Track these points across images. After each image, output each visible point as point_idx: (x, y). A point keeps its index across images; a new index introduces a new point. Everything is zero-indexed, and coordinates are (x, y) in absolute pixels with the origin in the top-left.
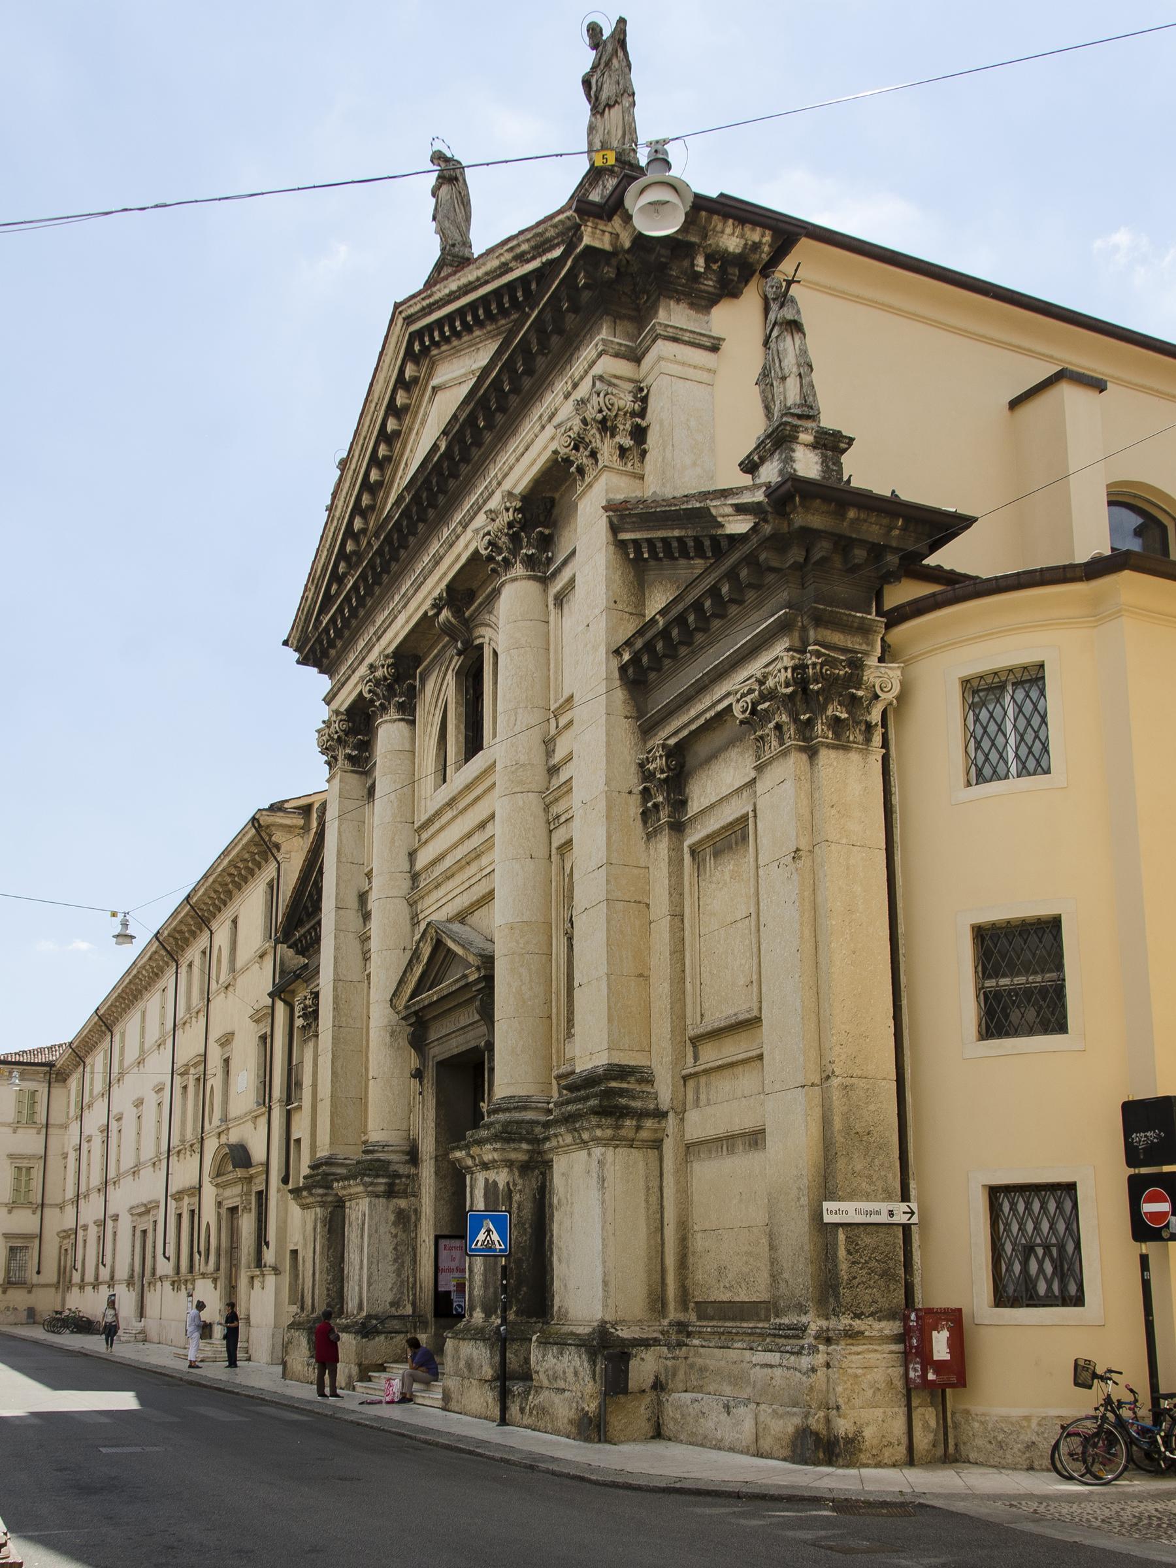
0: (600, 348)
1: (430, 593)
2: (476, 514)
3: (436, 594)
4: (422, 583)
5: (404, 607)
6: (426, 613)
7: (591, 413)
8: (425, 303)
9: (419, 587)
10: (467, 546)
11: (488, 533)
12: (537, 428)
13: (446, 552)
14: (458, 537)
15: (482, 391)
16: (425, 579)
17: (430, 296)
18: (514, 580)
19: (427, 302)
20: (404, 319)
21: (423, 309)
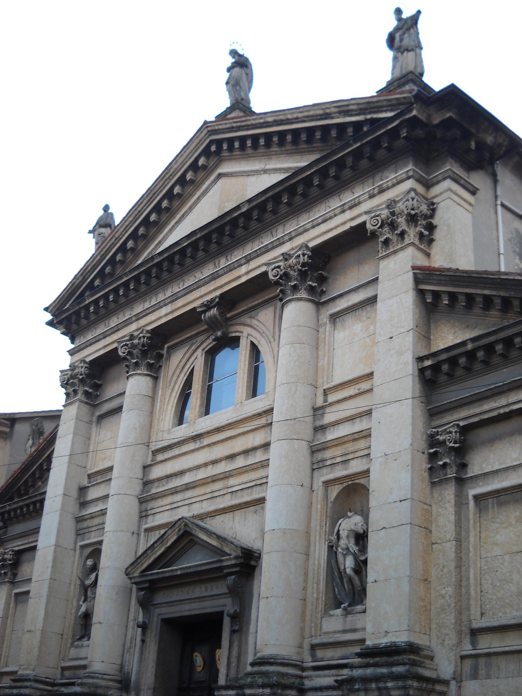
1: (201, 297)
3: (209, 298)
6: (194, 309)
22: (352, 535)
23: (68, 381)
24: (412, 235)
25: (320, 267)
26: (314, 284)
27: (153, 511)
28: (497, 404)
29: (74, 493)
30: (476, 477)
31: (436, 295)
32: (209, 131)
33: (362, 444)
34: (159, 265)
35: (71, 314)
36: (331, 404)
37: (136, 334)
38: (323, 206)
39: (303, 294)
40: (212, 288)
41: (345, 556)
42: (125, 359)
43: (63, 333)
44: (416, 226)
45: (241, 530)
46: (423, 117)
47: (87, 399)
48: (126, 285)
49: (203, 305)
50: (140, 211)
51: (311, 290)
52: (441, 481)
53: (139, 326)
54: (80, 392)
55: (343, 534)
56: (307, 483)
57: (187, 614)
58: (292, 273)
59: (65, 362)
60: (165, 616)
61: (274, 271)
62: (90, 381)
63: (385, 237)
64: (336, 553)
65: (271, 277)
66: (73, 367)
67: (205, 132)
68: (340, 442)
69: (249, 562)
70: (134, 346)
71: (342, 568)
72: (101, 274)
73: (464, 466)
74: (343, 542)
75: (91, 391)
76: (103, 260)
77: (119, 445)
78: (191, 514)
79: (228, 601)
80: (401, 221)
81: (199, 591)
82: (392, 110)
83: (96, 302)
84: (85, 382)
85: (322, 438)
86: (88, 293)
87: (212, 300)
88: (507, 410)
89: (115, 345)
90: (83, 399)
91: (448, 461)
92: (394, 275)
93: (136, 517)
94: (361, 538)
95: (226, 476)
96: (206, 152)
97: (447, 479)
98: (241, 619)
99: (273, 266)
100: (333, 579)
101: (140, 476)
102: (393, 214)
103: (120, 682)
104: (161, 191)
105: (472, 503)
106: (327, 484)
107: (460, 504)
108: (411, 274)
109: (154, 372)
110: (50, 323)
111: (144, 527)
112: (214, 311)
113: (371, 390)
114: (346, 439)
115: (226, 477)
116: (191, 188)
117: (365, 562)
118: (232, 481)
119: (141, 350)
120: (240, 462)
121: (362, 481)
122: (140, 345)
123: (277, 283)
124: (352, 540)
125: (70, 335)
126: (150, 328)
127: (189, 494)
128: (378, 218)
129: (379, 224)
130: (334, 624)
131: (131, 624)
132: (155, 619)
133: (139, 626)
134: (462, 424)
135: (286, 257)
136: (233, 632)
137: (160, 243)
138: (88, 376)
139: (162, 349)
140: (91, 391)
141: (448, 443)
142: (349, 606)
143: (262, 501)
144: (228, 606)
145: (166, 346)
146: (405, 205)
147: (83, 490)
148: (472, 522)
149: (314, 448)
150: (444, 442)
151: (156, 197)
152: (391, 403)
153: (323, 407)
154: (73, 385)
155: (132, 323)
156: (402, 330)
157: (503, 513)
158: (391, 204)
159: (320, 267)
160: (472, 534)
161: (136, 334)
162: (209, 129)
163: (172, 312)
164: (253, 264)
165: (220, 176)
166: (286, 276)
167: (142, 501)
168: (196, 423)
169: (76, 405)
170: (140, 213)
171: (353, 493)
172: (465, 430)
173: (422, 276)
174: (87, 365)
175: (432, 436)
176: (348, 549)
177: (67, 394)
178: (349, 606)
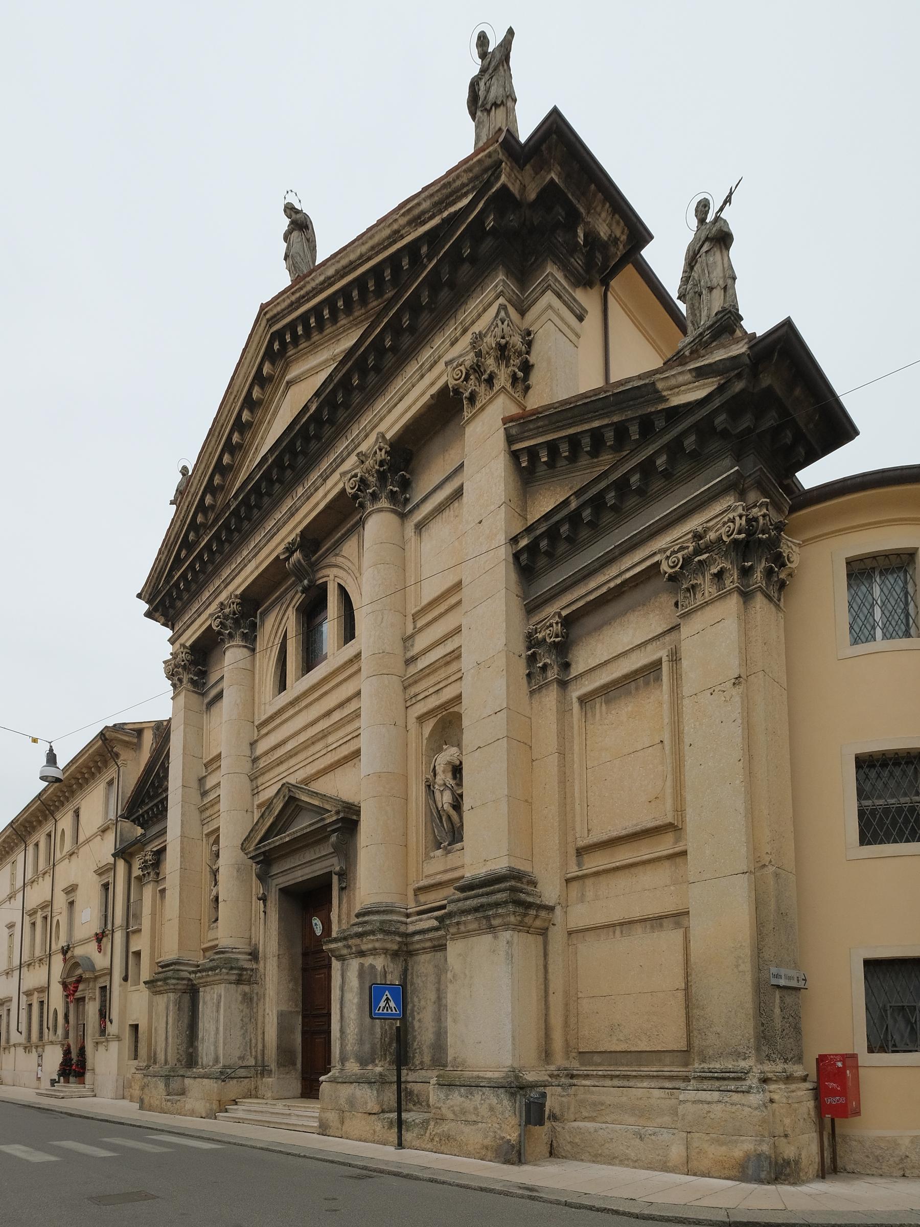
0: (500, 288)
1: (283, 540)
2: (349, 455)
3: (290, 539)
4: (275, 534)
6: (278, 557)
7: (490, 341)
8: (293, 298)
9: (272, 537)
10: (326, 495)
11: (355, 476)
12: (417, 376)
13: (303, 504)
14: (316, 490)
15: (362, 349)
16: (278, 530)
17: (301, 289)
18: (380, 510)
19: (298, 295)
20: (268, 320)
21: (292, 303)
22: (450, 768)
23: (173, 672)
24: (503, 378)
25: (402, 462)
26: (395, 489)
27: (263, 787)
29: (194, 784)
30: (581, 675)
31: (532, 452)
33: (454, 667)
35: (166, 597)
38: (399, 378)
39: (384, 503)
41: (442, 792)
44: (507, 366)
45: (342, 786)
47: (194, 687)
51: (393, 496)
52: (540, 688)
54: (185, 681)
56: (401, 723)
57: (300, 879)
58: (371, 478)
59: (166, 651)
60: (281, 886)
62: (194, 667)
66: (174, 655)
67: (264, 322)
68: (432, 669)
69: (348, 821)
70: (226, 617)
71: (440, 806)
73: (566, 666)
74: (440, 779)
75: (196, 678)
77: (224, 729)
79: (335, 860)
80: (490, 363)
81: (309, 855)
84: (190, 670)
85: (413, 670)
87: (293, 543)
88: (618, 581)
90: (190, 687)
91: (548, 661)
93: (249, 796)
94: (457, 770)
95: (324, 735)
97: (547, 684)
98: (346, 876)
100: (432, 821)
101: (248, 753)
103: (250, 954)
104: (229, 421)
105: (576, 706)
106: (421, 719)
107: (563, 711)
109: (250, 640)
110: (149, 615)
111: (256, 803)
112: (297, 555)
113: (459, 602)
114: (437, 664)
115: (325, 736)
117: (461, 796)
118: (330, 739)
119: (232, 618)
120: (336, 716)
121: (456, 709)
124: (450, 775)
126: (238, 592)
127: (292, 762)
130: (437, 866)
131: (254, 898)
132: (273, 890)
133: (259, 899)
136: (342, 889)
138: (191, 663)
140: (196, 678)
142: (449, 845)
143: (357, 753)
144: (334, 863)
147: (201, 780)
148: (576, 727)
149: (406, 683)
150: (544, 639)
151: (225, 431)
153: (412, 636)
155: (221, 592)
159: (402, 462)
160: (576, 741)
162: (268, 316)
163: (257, 568)
167: (253, 779)
169: (183, 694)
171: (447, 724)
172: (568, 622)
175: (529, 636)
177: (174, 685)
178: (449, 845)
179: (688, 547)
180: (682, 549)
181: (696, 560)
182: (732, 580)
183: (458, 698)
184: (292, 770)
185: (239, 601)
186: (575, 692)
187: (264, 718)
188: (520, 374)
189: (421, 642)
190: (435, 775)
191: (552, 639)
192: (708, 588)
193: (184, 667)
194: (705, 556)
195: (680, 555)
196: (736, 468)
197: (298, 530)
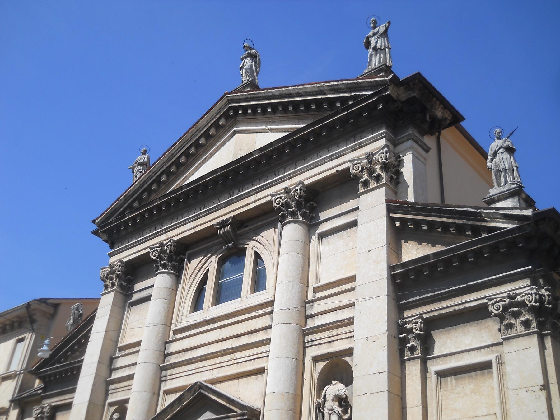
1: (218, 217)
3: (224, 218)
5: (194, 220)
6: (213, 226)
27: (172, 377)
28: (453, 302)
32: (228, 100)
34: (187, 194)
36: (319, 299)
37: (165, 242)
40: (227, 211)
42: (155, 261)
43: (106, 241)
46: (394, 95)
47: (122, 290)
48: (159, 207)
49: (219, 223)
50: (173, 154)
53: (168, 237)
55: (329, 398)
61: (277, 200)
63: (364, 179)
64: (323, 413)
65: (274, 204)
67: (226, 100)
72: (139, 198)
74: (329, 404)
76: (141, 188)
78: (205, 379)
82: (371, 90)
83: (134, 219)
86: (128, 211)
87: (227, 220)
89: (148, 250)
91: (414, 343)
92: (372, 206)
96: (226, 115)
99: (276, 197)
102: (370, 162)
104: (190, 141)
106: (317, 359)
108: (385, 205)
110: (95, 233)
116: (212, 140)
118: (237, 355)
120: (245, 340)
122: (168, 251)
123: (279, 210)
125: (110, 242)
128: (359, 165)
129: (360, 169)
134: (425, 316)
135: (287, 191)
137: (187, 178)
139: (185, 255)
141: (414, 331)
145: (188, 253)
146: (380, 156)
152: (369, 299)
153: (313, 301)
154: (111, 279)
156: (378, 245)
157: (460, 386)
158: (370, 156)
161: (165, 242)
163: (194, 228)
164: (260, 195)
165: (236, 132)
166: (287, 205)
168: (210, 310)
170: (173, 155)
173: (394, 206)
174: (124, 265)
176: (332, 410)
179: (505, 301)
180: (500, 301)
181: (511, 310)
182: (534, 327)
183: (350, 352)
184: (200, 370)
185: (175, 244)
186: (434, 367)
187: (180, 326)
188: (395, 177)
189: (317, 307)
190: (325, 401)
191: (417, 332)
192: (520, 329)
193: (118, 276)
194: (516, 309)
195: (500, 304)
196: (530, 267)
197: (232, 215)
